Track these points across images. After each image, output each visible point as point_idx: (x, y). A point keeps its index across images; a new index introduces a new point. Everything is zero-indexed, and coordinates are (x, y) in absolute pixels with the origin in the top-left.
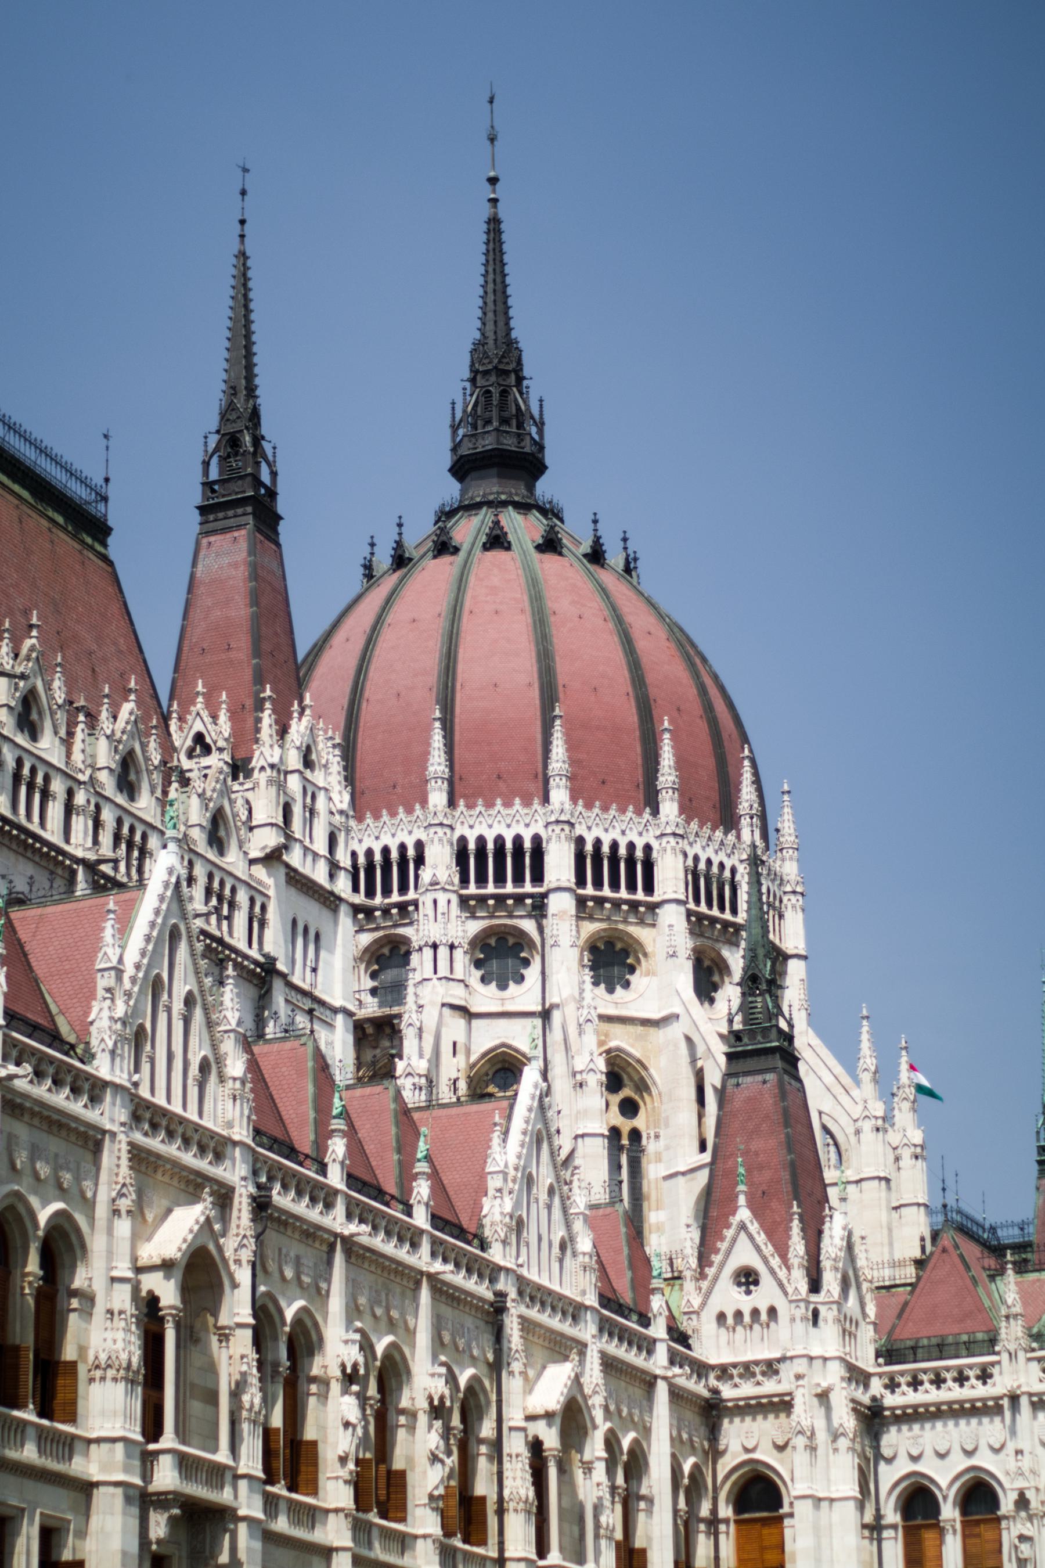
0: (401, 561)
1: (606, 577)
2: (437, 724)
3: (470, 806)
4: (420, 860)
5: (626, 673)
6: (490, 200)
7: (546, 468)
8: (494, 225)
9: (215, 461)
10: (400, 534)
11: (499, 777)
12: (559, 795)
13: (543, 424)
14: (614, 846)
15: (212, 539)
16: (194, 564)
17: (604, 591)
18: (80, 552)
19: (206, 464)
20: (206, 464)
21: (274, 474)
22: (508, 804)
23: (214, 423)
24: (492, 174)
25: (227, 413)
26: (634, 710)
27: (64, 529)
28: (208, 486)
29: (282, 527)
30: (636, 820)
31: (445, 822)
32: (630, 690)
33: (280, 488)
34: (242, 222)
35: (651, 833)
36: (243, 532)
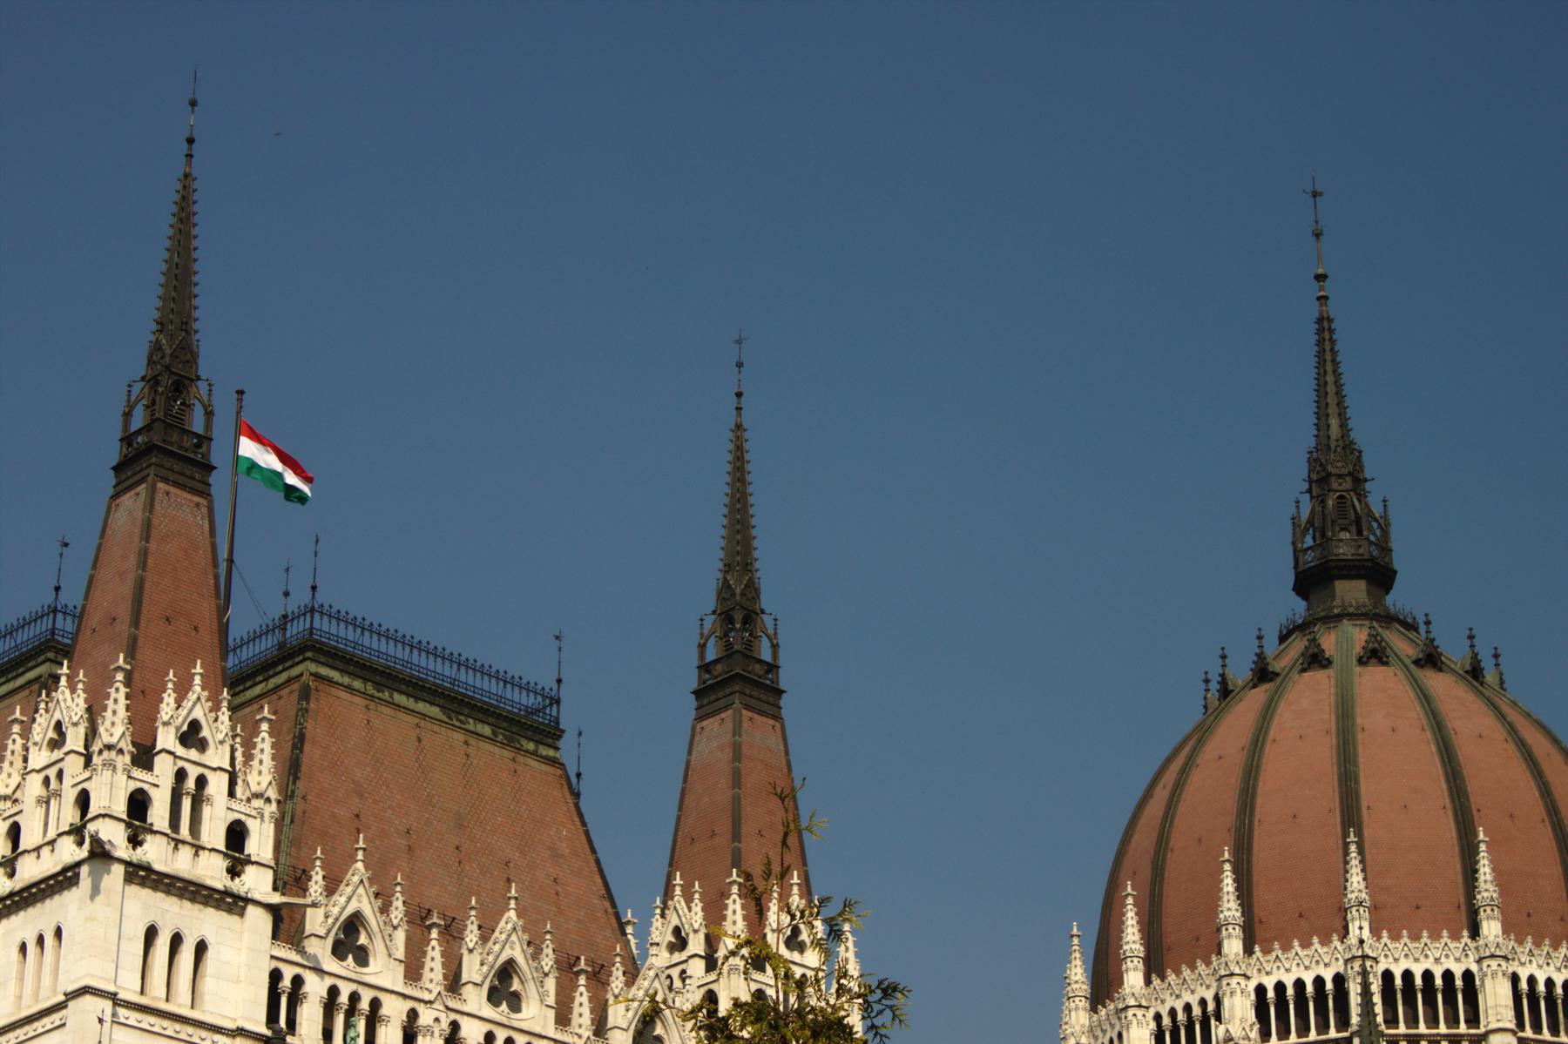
0: (1225, 692)
1: (1437, 683)
2: (1227, 866)
3: (1267, 951)
4: (1219, 1019)
5: (1444, 785)
6: (1319, 298)
7: (1395, 572)
8: (1324, 325)
9: (712, 641)
10: (1224, 666)
11: (1301, 915)
12: (1359, 927)
13: (1388, 525)
14: (1428, 975)
15: (705, 723)
16: (690, 753)
17: (1426, 699)
18: (513, 760)
19: (702, 647)
20: (702, 647)
21: (775, 647)
22: (1306, 945)
23: (711, 603)
24: (1320, 271)
25: (725, 591)
26: (1452, 824)
27: (492, 740)
28: (705, 668)
29: (784, 701)
30: (1452, 945)
31: (1237, 971)
32: (1448, 802)
33: (783, 661)
34: (739, 395)
35: (1471, 958)
36: (730, 712)
